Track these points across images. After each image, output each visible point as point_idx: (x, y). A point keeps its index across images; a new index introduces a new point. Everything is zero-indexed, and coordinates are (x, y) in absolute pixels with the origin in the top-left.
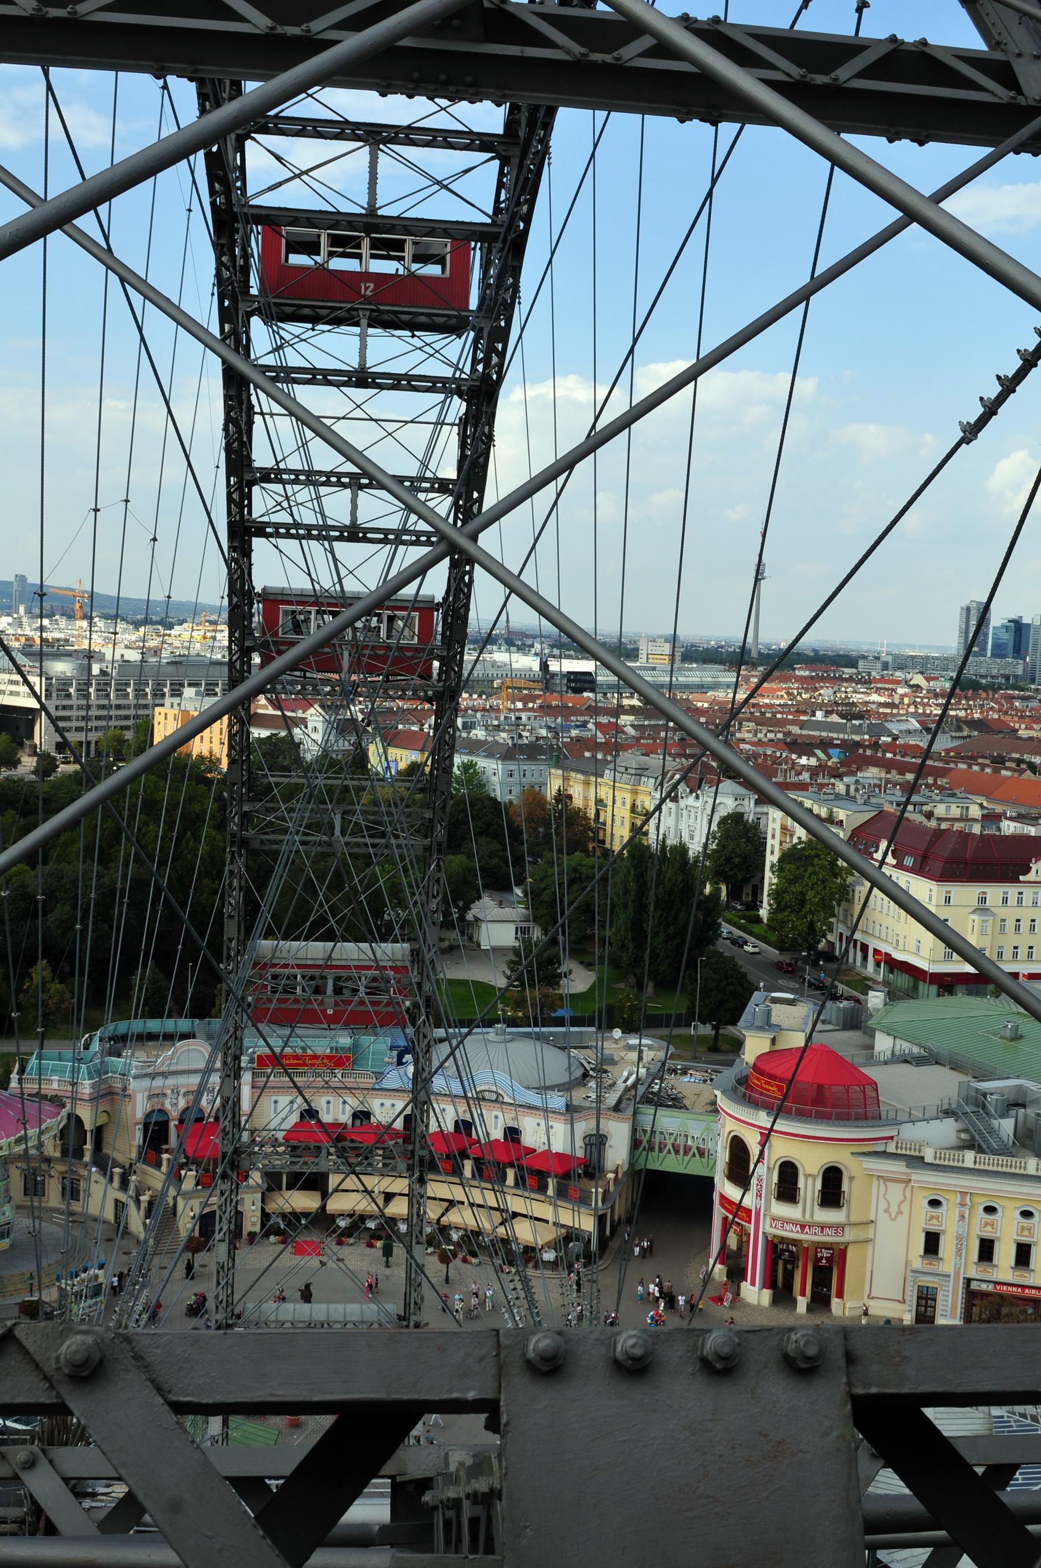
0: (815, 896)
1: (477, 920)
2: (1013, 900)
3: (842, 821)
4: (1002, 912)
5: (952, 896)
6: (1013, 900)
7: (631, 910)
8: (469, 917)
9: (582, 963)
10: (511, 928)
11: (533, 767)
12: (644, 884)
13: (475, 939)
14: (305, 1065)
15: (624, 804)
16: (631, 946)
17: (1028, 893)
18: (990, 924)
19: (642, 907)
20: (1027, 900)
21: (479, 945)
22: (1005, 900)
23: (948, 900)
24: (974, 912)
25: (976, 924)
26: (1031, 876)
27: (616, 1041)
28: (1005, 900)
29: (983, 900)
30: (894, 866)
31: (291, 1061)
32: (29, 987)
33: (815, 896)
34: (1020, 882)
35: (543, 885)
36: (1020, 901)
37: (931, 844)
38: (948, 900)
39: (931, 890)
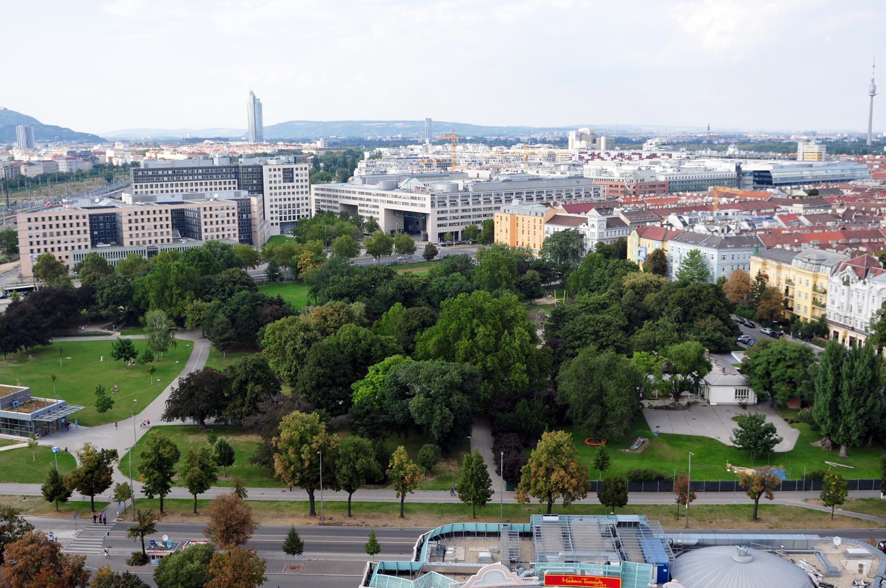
1: (707, 384)
7: (829, 394)
8: (702, 382)
9: (786, 420)
10: (732, 391)
11: (739, 253)
12: (839, 374)
13: (705, 397)
14: (583, 584)
15: (807, 284)
16: (829, 422)
19: (837, 393)
21: (709, 402)
27: (836, 547)
31: (572, 581)
32: (392, 466)
35: (756, 363)
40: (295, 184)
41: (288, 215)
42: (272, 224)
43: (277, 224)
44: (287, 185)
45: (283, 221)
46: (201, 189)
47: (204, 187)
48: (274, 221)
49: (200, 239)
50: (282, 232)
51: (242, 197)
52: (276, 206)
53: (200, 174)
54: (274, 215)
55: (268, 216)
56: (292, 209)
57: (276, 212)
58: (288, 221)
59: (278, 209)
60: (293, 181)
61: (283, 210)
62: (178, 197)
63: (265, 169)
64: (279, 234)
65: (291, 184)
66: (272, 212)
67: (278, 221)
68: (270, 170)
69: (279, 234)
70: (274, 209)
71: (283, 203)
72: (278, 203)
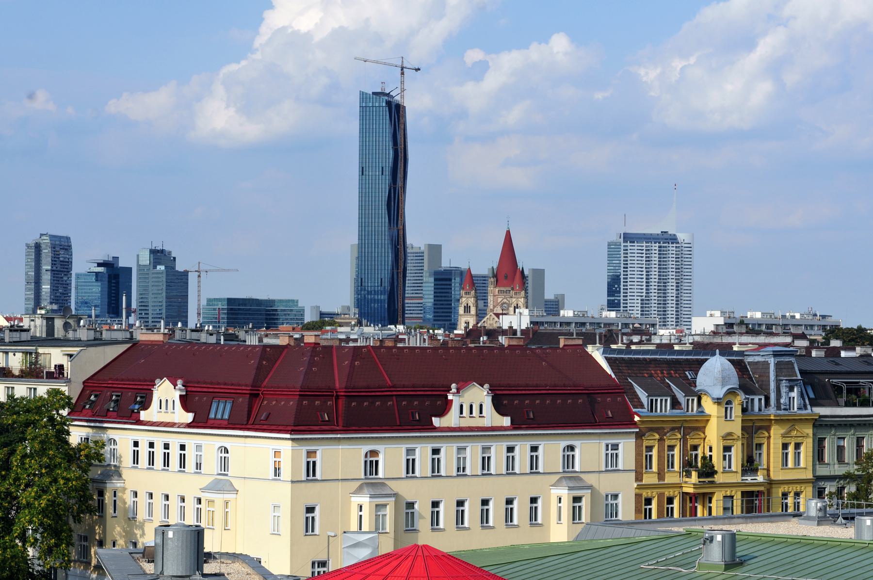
0: (38, 497)
2: (423, 466)
3: (60, 368)
4: (408, 490)
5: (318, 459)
6: (423, 466)
17: (448, 453)
18: (389, 511)
20: (447, 464)
22: (410, 465)
23: (311, 468)
24: (359, 491)
25: (365, 513)
26: (451, 419)
28: (410, 465)
29: (372, 467)
30: (189, 426)
33: (38, 497)
34: (435, 429)
36: (435, 465)
37: (261, 372)
38: (311, 468)
39: (277, 453)
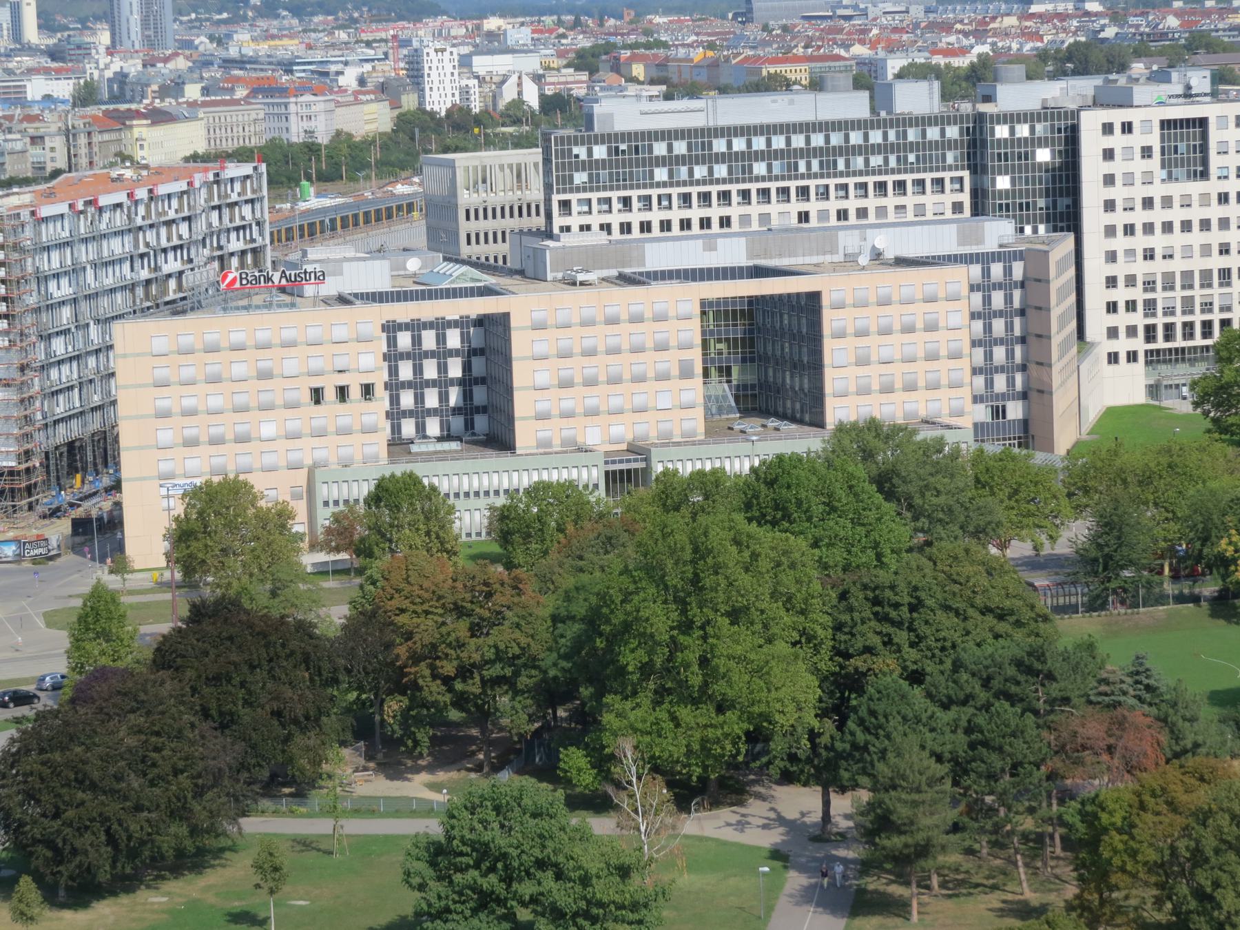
40: (1213, 186)
41: (1179, 319)
42: (1113, 358)
43: (1132, 357)
44: (1177, 189)
45: (1161, 344)
46: (823, 215)
47: (833, 205)
48: (1123, 345)
49: (818, 422)
50: (1153, 390)
51: (990, 246)
52: (1131, 281)
53: (877, 149)
54: (1122, 319)
55: (1097, 322)
56: (1197, 293)
57: (1131, 306)
58: (1179, 343)
59: (1138, 294)
60: (1204, 175)
61: (1159, 295)
62: (733, 252)
63: (1091, 123)
64: (1139, 397)
65: (1195, 188)
66: (1112, 307)
67: (1139, 344)
68: (1108, 129)
69: (1139, 397)
70: (1121, 295)
71: (1158, 267)
72: (1141, 268)
